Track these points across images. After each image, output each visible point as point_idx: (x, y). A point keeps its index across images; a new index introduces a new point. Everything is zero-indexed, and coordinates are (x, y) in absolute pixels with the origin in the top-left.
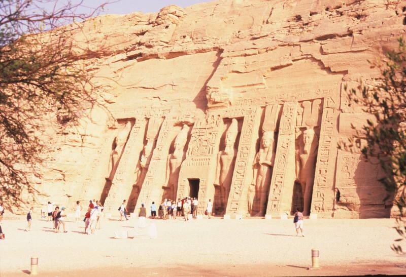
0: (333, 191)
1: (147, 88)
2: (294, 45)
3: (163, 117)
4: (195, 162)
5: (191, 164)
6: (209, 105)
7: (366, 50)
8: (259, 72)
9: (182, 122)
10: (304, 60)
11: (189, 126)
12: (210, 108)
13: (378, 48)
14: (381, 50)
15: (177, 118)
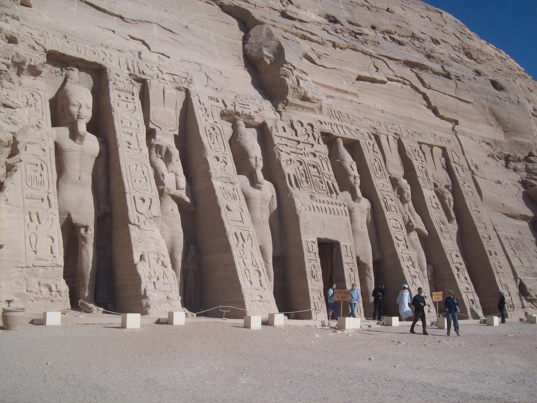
0: (514, 282)
1: (104, 11)
2: (371, 56)
3: (179, 89)
4: (323, 206)
5: (316, 209)
6: (290, 98)
7: (472, 103)
8: (342, 74)
9: (237, 114)
10: (399, 85)
11: (248, 126)
12: (292, 104)
13: (484, 107)
14: (487, 109)
15: (220, 101)
